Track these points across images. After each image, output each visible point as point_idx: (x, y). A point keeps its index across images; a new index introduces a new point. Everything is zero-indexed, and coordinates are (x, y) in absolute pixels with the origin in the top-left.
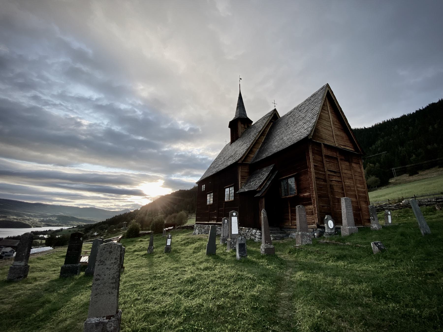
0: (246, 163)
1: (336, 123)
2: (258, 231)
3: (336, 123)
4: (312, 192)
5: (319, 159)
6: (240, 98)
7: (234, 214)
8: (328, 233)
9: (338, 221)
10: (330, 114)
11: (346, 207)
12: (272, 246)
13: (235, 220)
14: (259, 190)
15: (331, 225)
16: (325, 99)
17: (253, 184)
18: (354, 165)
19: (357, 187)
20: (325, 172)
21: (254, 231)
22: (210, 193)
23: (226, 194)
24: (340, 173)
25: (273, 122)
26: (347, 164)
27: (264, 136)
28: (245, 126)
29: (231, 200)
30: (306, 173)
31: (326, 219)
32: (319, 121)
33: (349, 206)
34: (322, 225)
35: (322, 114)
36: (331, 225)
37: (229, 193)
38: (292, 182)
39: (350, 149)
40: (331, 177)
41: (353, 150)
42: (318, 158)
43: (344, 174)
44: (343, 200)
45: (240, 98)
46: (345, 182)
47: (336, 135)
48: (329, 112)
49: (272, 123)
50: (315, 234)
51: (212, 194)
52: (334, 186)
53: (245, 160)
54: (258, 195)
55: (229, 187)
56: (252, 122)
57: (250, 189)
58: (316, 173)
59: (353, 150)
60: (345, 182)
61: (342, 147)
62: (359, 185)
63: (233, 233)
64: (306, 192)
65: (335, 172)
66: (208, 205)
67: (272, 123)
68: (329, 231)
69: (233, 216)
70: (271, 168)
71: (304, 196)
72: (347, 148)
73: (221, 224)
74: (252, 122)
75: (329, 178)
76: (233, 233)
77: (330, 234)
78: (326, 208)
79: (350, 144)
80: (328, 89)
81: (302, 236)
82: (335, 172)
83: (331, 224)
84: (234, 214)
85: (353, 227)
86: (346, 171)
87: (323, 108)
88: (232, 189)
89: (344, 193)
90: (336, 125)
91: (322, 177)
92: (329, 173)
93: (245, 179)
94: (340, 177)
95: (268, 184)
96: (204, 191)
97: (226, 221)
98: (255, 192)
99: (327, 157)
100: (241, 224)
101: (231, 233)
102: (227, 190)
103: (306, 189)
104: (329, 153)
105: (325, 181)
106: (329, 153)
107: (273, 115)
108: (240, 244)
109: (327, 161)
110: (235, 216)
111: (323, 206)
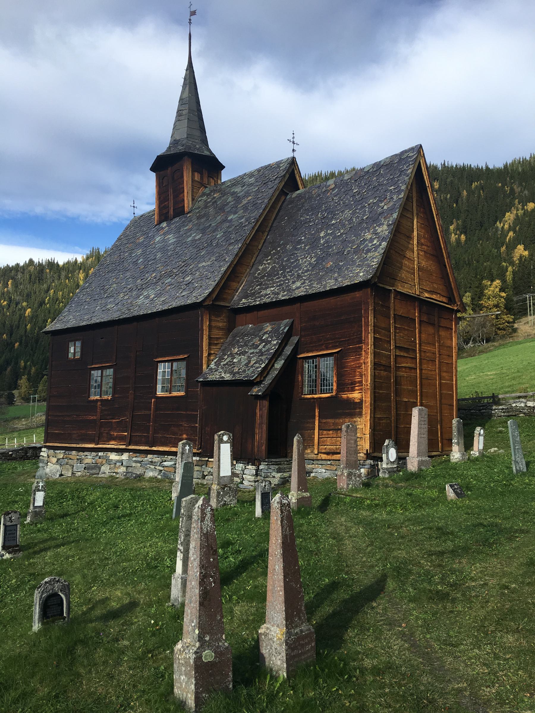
0: (222, 304)
1: (423, 241)
2: (250, 467)
5: (383, 325)
6: (190, 81)
7: (225, 438)
8: (387, 469)
9: (403, 447)
11: (419, 424)
12: (307, 494)
13: (226, 450)
14: (258, 380)
15: (392, 457)
16: (412, 185)
22: (102, 368)
23: (159, 377)
28: (202, 178)
29: (175, 394)
30: (358, 351)
31: (387, 446)
33: (423, 423)
34: (376, 454)
36: (392, 457)
37: (167, 377)
38: (327, 366)
40: (399, 359)
41: (444, 300)
44: (415, 412)
45: (190, 81)
47: (419, 268)
51: (110, 372)
52: (402, 379)
53: (217, 298)
54: (255, 390)
56: (222, 167)
57: (237, 377)
58: (376, 354)
59: (444, 300)
61: (427, 295)
63: (221, 475)
64: (353, 390)
65: (407, 350)
68: (389, 466)
69: (221, 441)
70: (284, 326)
71: (348, 397)
72: (434, 297)
73: (175, 454)
74: (222, 167)
76: (221, 475)
77: (391, 471)
79: (441, 287)
81: (350, 475)
83: (392, 454)
84: (225, 438)
85: (424, 459)
88: (181, 368)
90: (422, 244)
91: (383, 362)
97: (187, 448)
98: (250, 384)
100: (236, 457)
101: (219, 474)
102: (163, 369)
107: (287, 176)
108: (262, 494)
110: (226, 442)
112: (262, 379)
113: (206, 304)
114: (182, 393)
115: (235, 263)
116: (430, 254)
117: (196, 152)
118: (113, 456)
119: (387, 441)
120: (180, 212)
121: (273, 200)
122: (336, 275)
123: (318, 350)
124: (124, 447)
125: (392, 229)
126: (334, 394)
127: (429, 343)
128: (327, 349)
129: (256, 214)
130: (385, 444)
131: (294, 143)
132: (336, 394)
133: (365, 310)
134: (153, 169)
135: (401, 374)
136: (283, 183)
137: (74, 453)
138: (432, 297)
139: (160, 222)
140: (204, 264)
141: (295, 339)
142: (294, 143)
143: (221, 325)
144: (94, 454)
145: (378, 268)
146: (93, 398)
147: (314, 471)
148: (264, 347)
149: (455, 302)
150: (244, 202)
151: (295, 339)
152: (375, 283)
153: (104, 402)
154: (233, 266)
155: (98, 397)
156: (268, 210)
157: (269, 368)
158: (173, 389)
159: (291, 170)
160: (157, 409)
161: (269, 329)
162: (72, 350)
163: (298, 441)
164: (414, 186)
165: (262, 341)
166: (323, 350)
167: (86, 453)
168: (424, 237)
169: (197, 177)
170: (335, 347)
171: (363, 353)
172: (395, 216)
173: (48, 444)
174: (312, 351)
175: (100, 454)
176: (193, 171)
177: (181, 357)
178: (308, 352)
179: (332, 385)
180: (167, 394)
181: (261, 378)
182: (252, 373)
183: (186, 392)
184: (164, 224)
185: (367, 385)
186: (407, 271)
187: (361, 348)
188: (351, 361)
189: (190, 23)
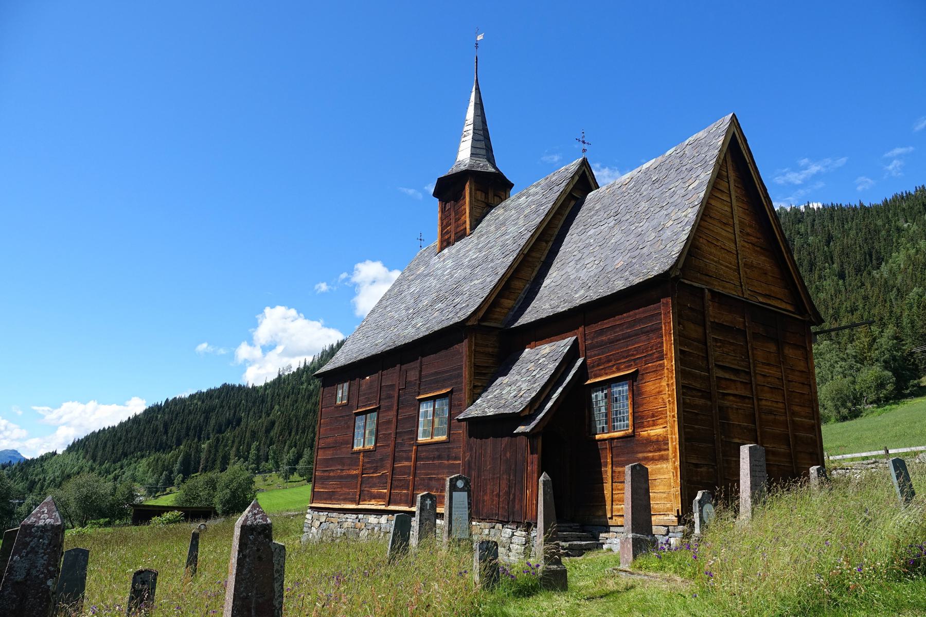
0: (492, 324)
1: (748, 230)
2: (518, 533)
3: (748, 230)
4: (673, 427)
10: (734, 201)
14: (527, 413)
16: (725, 159)
17: (509, 393)
18: (789, 352)
19: (794, 414)
20: (708, 370)
21: (507, 532)
24: (749, 373)
25: (576, 199)
26: (772, 348)
27: (547, 242)
28: (487, 197)
29: (437, 438)
32: (703, 223)
33: (758, 469)
35: (713, 202)
39: (783, 306)
41: (789, 308)
42: (694, 331)
43: (760, 378)
46: (759, 400)
47: (745, 265)
48: (733, 197)
49: (573, 203)
50: (672, 541)
53: (484, 319)
55: (434, 399)
57: (502, 411)
59: (789, 308)
60: (759, 400)
61: (761, 299)
62: (797, 409)
64: (654, 424)
65: (736, 372)
66: (359, 452)
67: (573, 203)
71: (649, 435)
75: (719, 387)
78: (704, 469)
80: (734, 129)
82: (736, 372)
86: (766, 370)
87: (714, 187)
89: (755, 431)
90: (748, 234)
92: (721, 374)
93: (485, 374)
94: (748, 384)
95: (555, 396)
96: (343, 406)
99: (719, 327)
102: (426, 409)
103: (655, 418)
104: (726, 318)
105: (707, 395)
106: (726, 318)
107: (577, 178)
109: (716, 340)
110: (462, 490)
111: (696, 465)
112: (532, 412)
113: (469, 323)
114: (444, 438)
115: (509, 276)
116: (761, 248)
117: (479, 169)
118: (372, 519)
119: (699, 495)
120: (461, 235)
121: (559, 204)
122: (627, 273)
123: (606, 374)
124: (383, 507)
125: (699, 212)
126: (630, 431)
127: (768, 365)
128: (619, 370)
129: (539, 220)
130: (698, 498)
131: (584, 142)
132: (634, 431)
133: (665, 314)
134: (436, 194)
135: (727, 403)
136: (571, 186)
137: (335, 514)
138: (769, 302)
139: (442, 249)
140: (476, 282)
141: (580, 362)
142: (584, 142)
143: (490, 350)
144: (355, 516)
145: (679, 257)
146: (356, 448)
147: (608, 541)
148: (538, 373)
149: (807, 312)
150: (527, 212)
151: (580, 362)
152: (677, 278)
153: (366, 452)
154: (506, 279)
155: (361, 447)
156: (551, 215)
157: (542, 399)
158: (435, 432)
159: (581, 172)
160: (416, 460)
161: (547, 351)
162: (340, 395)
163: (545, 483)
164: (729, 159)
165: (536, 366)
166: (614, 372)
167: (347, 516)
168: (751, 226)
169: (480, 196)
170: (628, 367)
171: (666, 371)
172: (702, 195)
173: (313, 505)
174: (600, 376)
175: (361, 516)
176: (476, 190)
177: (444, 391)
178: (596, 376)
179: (628, 419)
180: (428, 439)
181: (530, 410)
182: (518, 406)
183: (449, 435)
184: (446, 251)
185: (674, 417)
186: (727, 267)
187: (662, 366)
188: (650, 387)
189: (477, 47)
